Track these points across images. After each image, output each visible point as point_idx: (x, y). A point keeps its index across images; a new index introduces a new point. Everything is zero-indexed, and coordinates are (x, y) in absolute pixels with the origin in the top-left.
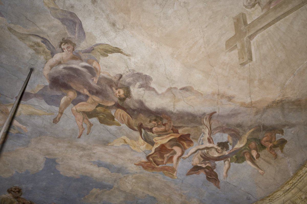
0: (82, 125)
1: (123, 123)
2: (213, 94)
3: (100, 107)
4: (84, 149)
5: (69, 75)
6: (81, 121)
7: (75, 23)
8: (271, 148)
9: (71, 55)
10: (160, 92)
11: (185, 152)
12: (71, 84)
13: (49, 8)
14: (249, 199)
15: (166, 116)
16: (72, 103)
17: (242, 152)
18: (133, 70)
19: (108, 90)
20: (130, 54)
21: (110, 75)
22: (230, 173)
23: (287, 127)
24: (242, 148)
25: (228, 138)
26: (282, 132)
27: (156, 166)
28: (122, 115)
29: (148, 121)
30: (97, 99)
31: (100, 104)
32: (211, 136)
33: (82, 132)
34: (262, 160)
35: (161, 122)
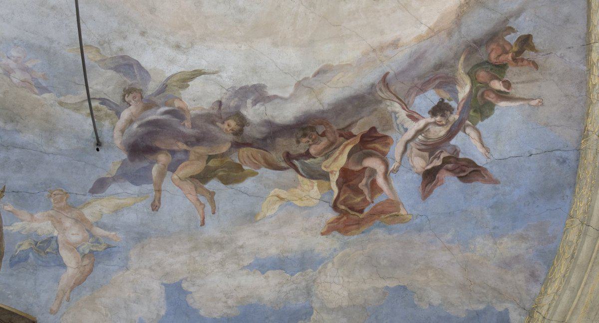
0: (198, 200)
1: (259, 168)
2: (366, 54)
3: (212, 160)
4: (219, 245)
5: (149, 133)
6: (194, 193)
7: (131, 66)
8: (514, 59)
9: (140, 105)
10: (287, 95)
11: (390, 161)
12: (157, 144)
13: (96, 61)
14: (564, 161)
15: (316, 120)
16: (169, 170)
17: (478, 97)
18: (233, 88)
19: (212, 130)
20: (217, 70)
21: (203, 109)
22: (489, 141)
23: (511, 20)
24: (471, 92)
25: (439, 94)
26: (511, 30)
27: (361, 216)
28: (250, 156)
29: (295, 143)
30: (202, 150)
31: (210, 156)
32: (411, 109)
33: (203, 212)
34: (520, 86)
35: (315, 133)
